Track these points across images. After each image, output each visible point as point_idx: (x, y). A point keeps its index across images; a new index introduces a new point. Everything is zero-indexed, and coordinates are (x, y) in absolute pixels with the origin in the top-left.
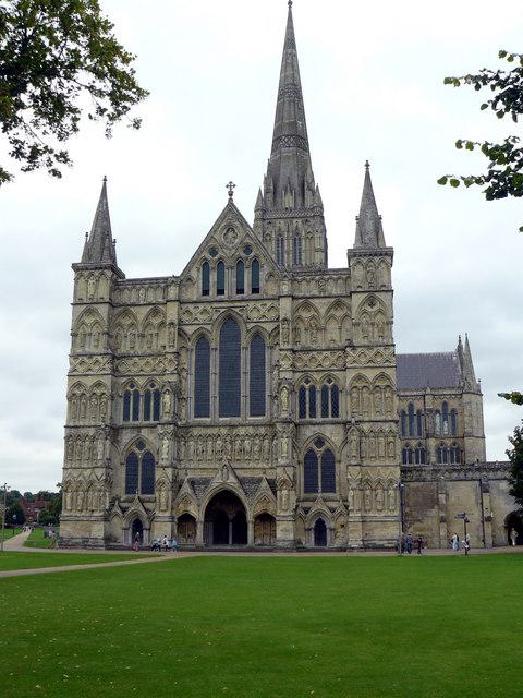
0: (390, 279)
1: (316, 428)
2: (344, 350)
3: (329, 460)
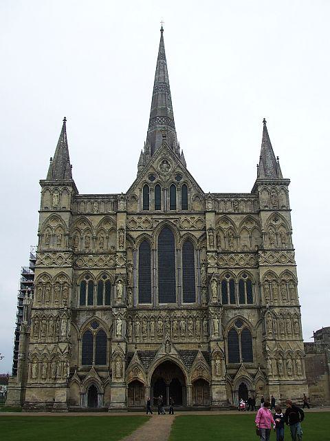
0: (288, 202)
1: (237, 311)
2: (257, 253)
3: (247, 335)
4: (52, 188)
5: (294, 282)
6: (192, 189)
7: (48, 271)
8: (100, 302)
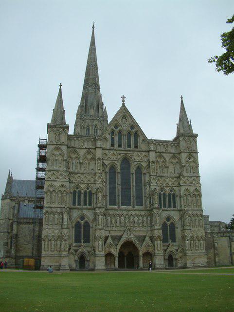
1: (167, 212)
2: (179, 177)
3: (173, 227)
4: (55, 129)
5: (200, 196)
6: (141, 136)
7: (54, 183)
8: (85, 204)
